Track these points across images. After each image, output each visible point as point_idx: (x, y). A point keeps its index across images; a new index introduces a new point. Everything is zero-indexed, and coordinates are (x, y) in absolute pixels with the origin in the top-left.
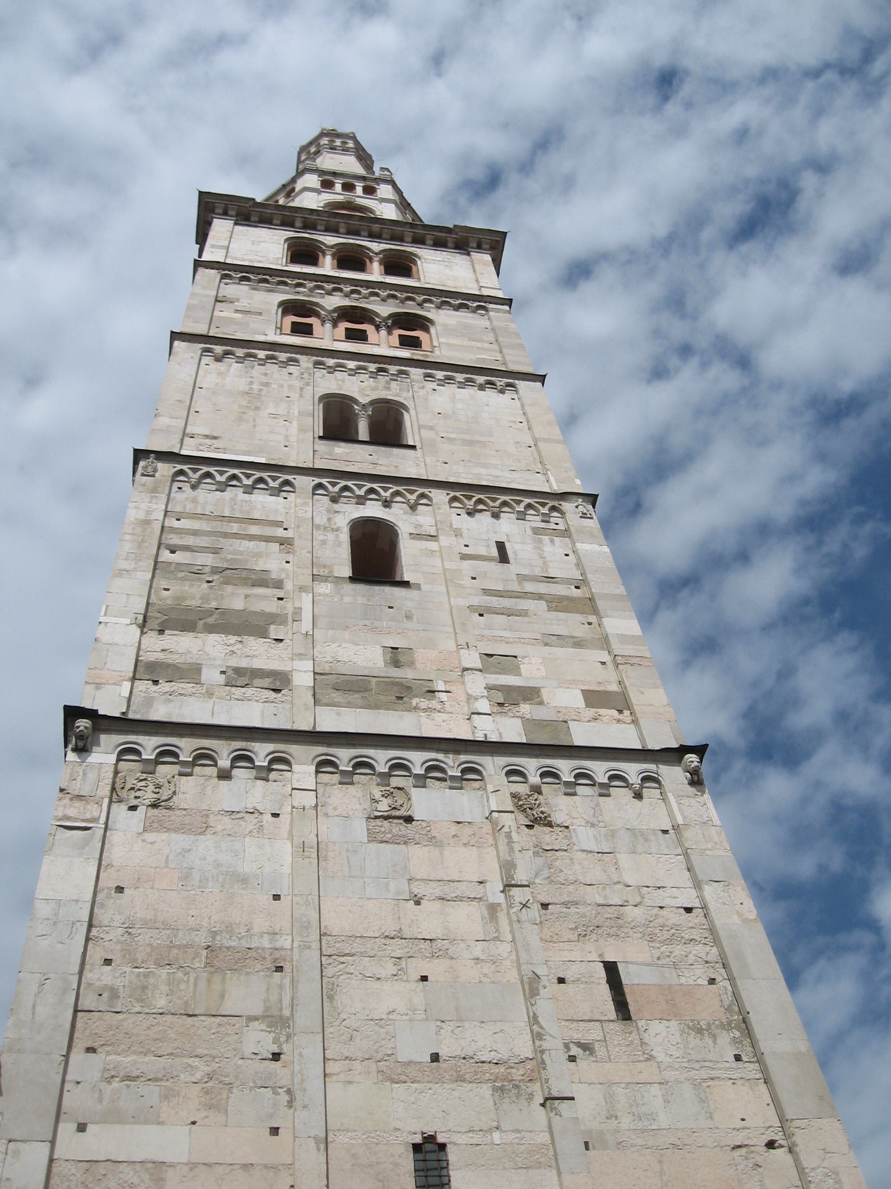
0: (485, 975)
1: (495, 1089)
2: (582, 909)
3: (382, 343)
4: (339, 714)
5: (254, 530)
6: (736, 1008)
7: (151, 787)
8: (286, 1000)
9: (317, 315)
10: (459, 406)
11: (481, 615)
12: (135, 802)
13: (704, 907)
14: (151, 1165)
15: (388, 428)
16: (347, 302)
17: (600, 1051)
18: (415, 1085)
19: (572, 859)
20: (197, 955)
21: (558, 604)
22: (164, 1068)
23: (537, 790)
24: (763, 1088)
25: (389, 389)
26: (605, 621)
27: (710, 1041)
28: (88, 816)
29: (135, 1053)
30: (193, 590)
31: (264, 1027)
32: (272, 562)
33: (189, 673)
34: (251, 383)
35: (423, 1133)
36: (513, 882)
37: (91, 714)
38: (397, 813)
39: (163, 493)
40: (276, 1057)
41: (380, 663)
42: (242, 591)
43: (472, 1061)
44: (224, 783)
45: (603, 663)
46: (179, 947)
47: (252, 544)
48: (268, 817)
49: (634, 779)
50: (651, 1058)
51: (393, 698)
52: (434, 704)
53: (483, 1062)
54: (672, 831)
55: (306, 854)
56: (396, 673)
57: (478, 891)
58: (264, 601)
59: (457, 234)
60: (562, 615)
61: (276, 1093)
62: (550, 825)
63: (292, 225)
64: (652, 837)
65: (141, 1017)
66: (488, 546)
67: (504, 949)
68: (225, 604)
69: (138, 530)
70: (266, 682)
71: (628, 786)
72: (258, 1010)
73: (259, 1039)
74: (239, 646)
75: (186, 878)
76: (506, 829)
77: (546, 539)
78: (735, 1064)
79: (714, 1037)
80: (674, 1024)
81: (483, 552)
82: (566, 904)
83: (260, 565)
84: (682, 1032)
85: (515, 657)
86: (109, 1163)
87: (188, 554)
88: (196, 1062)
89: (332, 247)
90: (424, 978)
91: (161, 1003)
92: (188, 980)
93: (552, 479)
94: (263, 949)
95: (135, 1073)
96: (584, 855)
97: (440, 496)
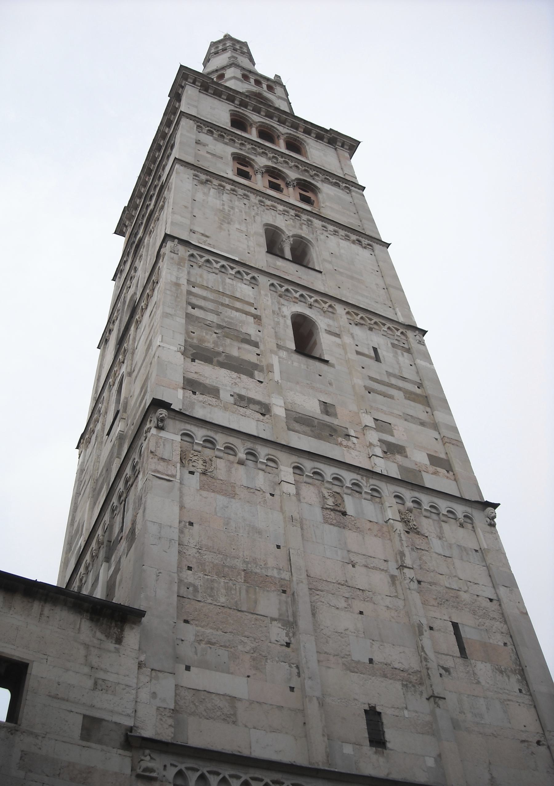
0: (393, 617)
1: (403, 685)
3: (291, 196)
4: (299, 438)
5: (238, 305)
6: (518, 663)
7: (201, 462)
8: (290, 613)
9: (252, 166)
10: (342, 251)
11: (369, 393)
12: (192, 469)
13: (499, 600)
14: (228, 698)
15: (300, 254)
16: (270, 163)
17: (454, 674)
18: (362, 675)
19: (431, 557)
20: (239, 574)
22: (229, 641)
23: (410, 510)
24: (533, 710)
25: (302, 229)
26: (436, 413)
27: (506, 678)
29: (211, 628)
31: (280, 625)
32: (250, 328)
34: (223, 205)
35: (369, 704)
36: (405, 565)
37: (166, 406)
38: (338, 509)
39: (184, 267)
40: (288, 645)
41: (318, 411)
42: (236, 344)
43: (390, 667)
44: (241, 468)
45: (437, 439)
46: (228, 567)
47: (238, 314)
49: (460, 515)
50: (478, 683)
51: (328, 434)
53: (396, 669)
54: (479, 551)
55: (294, 523)
56: (327, 419)
57: (383, 566)
58: (248, 354)
59: (331, 135)
60: (412, 403)
61: (290, 666)
62: (418, 533)
64: (470, 553)
65: (212, 607)
66: (368, 349)
67: (401, 603)
68: (228, 350)
69: (174, 289)
70: (257, 407)
72: (276, 615)
73: (277, 633)
74: (238, 380)
75: (227, 524)
76: (398, 532)
78: (519, 694)
79: (508, 677)
80: (488, 665)
81: (366, 351)
82: (431, 584)
85: (390, 424)
86: (205, 693)
87: (202, 311)
88: (245, 640)
89: (257, 123)
90: (361, 613)
91: (222, 600)
93: (399, 314)
94: (275, 578)
95: (214, 640)
96: (436, 555)
97: (340, 309)
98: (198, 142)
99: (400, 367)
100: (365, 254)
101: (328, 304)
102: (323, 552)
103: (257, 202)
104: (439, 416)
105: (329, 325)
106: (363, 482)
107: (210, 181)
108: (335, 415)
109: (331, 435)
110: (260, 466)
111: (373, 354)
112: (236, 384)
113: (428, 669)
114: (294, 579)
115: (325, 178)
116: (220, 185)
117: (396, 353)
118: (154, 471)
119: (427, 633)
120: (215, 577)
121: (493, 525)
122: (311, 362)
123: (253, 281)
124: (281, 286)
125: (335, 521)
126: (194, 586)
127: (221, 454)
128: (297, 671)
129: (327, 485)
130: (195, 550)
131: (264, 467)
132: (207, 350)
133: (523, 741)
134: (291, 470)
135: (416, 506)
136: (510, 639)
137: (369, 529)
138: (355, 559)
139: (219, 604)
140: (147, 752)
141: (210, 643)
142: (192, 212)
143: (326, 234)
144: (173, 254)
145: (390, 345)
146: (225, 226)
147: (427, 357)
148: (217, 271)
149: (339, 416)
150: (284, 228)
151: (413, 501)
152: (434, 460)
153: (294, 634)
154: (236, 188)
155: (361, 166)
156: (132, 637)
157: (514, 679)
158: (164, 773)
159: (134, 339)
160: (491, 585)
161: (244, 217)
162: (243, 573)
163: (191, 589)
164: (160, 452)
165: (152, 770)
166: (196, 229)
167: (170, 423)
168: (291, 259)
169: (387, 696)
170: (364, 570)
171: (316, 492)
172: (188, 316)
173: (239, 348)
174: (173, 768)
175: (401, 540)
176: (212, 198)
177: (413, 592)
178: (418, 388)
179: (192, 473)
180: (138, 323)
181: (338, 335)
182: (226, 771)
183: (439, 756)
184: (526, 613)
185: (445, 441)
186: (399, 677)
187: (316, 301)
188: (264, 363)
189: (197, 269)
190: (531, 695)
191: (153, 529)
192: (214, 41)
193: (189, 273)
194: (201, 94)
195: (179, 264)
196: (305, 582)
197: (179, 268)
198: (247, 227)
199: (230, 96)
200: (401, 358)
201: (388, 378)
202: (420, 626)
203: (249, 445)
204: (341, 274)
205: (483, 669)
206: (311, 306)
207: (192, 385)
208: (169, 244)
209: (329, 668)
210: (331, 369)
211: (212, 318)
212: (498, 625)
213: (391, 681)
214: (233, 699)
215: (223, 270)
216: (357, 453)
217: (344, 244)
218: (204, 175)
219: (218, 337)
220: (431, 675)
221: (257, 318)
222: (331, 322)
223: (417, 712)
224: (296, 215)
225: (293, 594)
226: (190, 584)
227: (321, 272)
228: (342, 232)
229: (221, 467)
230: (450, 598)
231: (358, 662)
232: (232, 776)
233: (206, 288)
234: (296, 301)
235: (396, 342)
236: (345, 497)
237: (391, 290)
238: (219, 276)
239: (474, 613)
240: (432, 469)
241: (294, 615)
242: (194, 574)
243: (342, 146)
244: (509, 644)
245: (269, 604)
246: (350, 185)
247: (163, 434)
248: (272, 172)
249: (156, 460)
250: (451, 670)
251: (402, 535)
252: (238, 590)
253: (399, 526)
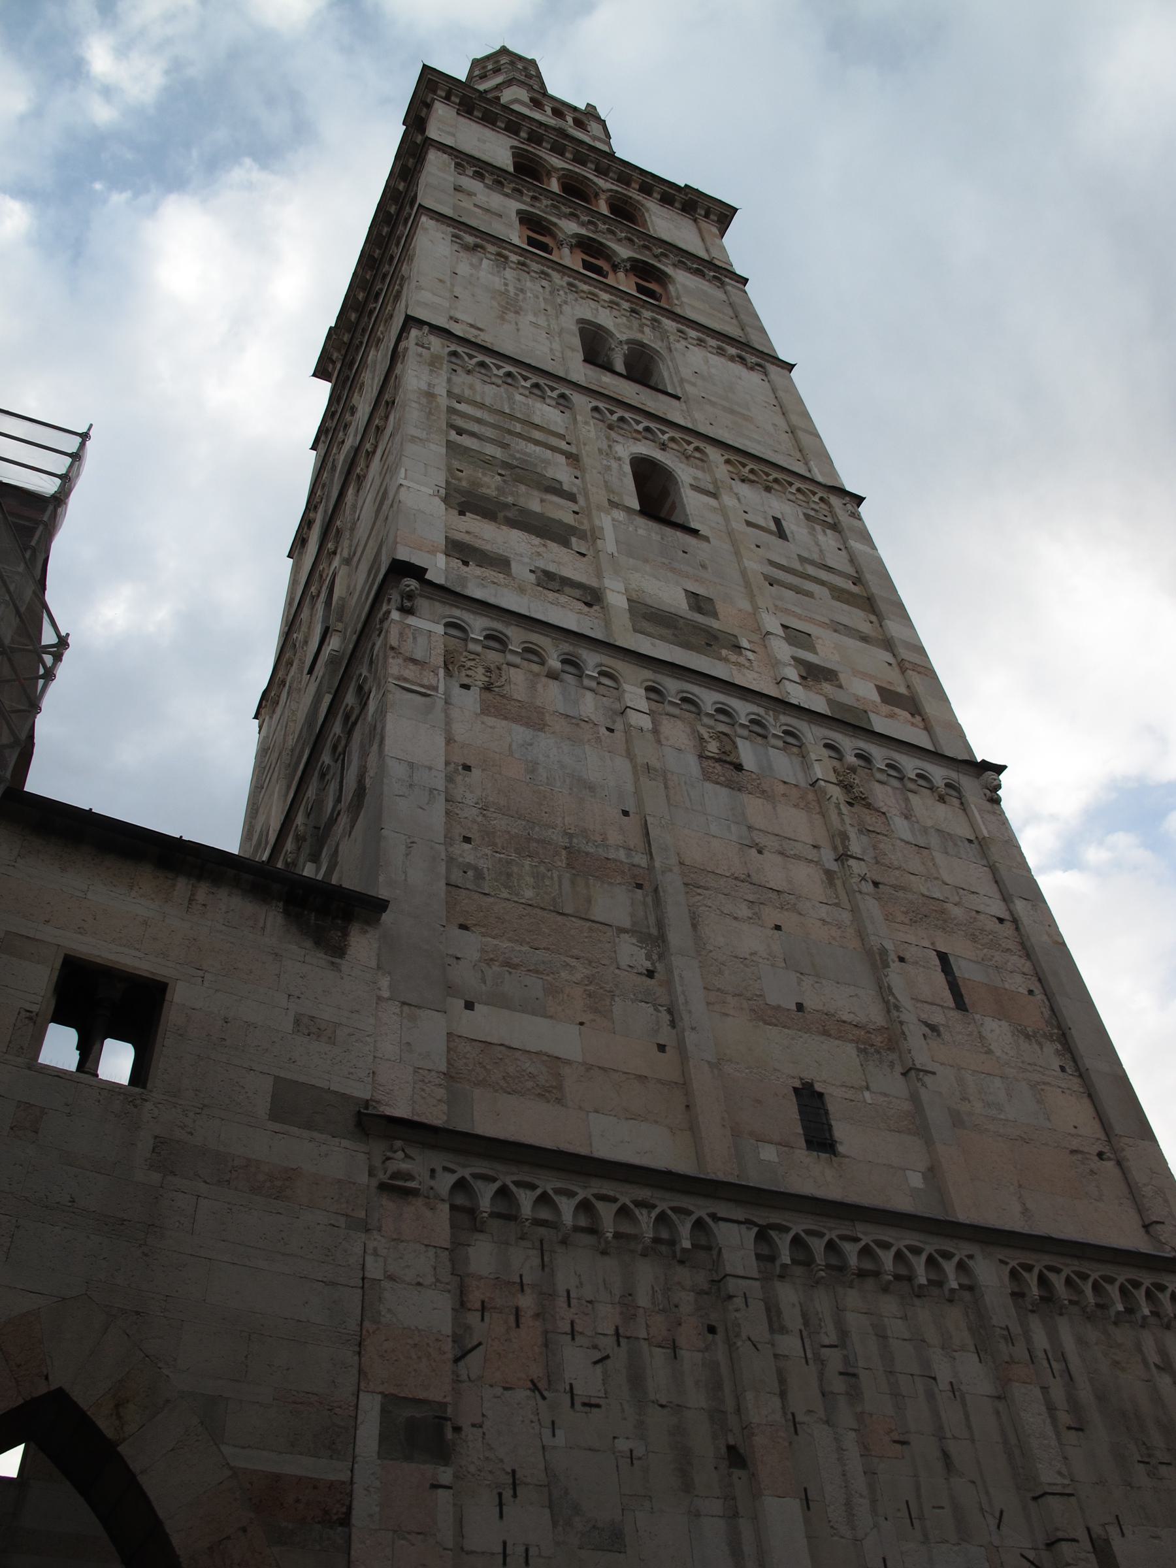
0: (834, 938)
1: (859, 1050)
2: (910, 896)
5: (537, 435)
6: (1055, 1023)
7: (481, 670)
8: (652, 920)
9: (553, 236)
10: (713, 371)
12: (466, 681)
13: (1015, 921)
14: (545, 1058)
16: (583, 231)
18: (786, 1031)
21: (839, 594)
22: (544, 962)
23: (853, 770)
24: (1086, 1101)
25: (643, 332)
27: (1036, 1047)
28: (425, 682)
29: (510, 940)
31: (634, 941)
32: (561, 472)
34: (506, 285)
35: (801, 1079)
37: (418, 572)
38: (728, 759)
39: (441, 369)
40: (650, 974)
44: (554, 686)
45: (890, 664)
46: (537, 841)
47: (538, 449)
48: (603, 731)
50: (989, 1052)
52: (742, 660)
53: (844, 1022)
54: (976, 842)
57: (812, 854)
58: (561, 511)
59: (686, 195)
60: (845, 607)
61: (656, 1010)
62: (868, 806)
63: (516, 133)
64: (960, 843)
66: (765, 518)
67: (846, 917)
68: (522, 502)
69: (424, 401)
70: (578, 593)
71: (932, 788)
72: (627, 924)
73: (631, 953)
74: (541, 549)
76: (834, 800)
78: (1061, 1074)
80: (1004, 1023)
81: (762, 523)
82: (895, 887)
83: (550, 473)
86: (502, 1048)
87: (475, 440)
88: (573, 962)
90: (778, 928)
91: (529, 893)
92: (552, 878)
94: (621, 862)
95: (516, 961)
96: (903, 844)
97: (714, 455)
98: (458, 189)
99: (821, 551)
100: (755, 377)
101: (692, 446)
102: (702, 826)
103: (565, 284)
104: (893, 628)
105: (695, 478)
106: (769, 719)
107: (482, 247)
108: (715, 615)
110: (586, 682)
111: (773, 527)
112: (539, 554)
113: (901, 1023)
114: (657, 864)
115: (680, 261)
116: (499, 254)
117: (814, 529)
118: (398, 679)
119: (895, 965)
120: (514, 856)
121: (997, 801)
122: (668, 531)
123: (562, 401)
124: (612, 413)
125: (723, 779)
126: (476, 869)
127: (517, 660)
128: (668, 1017)
129: (706, 720)
130: (475, 811)
131: (593, 684)
132: (486, 498)
133: (1073, 1152)
134: (642, 692)
135: (862, 763)
136: (1038, 984)
137: (784, 795)
139: (523, 901)
140: (398, 1144)
141: (507, 964)
142: (452, 291)
143: (684, 343)
144: (420, 349)
145: (801, 516)
146: (510, 316)
147: (866, 538)
148: (499, 382)
149: (720, 617)
150: (612, 329)
151: (857, 755)
152: (887, 695)
153: (661, 956)
154: (528, 261)
155: (738, 246)
156: (362, 946)
157: (1050, 1048)
158: (432, 1183)
159: (354, 506)
160: (998, 896)
161: (543, 305)
162: (564, 852)
163: (470, 873)
164: (407, 648)
165: (409, 1177)
166: (459, 316)
167: (422, 604)
168: (624, 373)
169: (833, 1067)
170: (779, 859)
171: (688, 730)
172: (450, 445)
173: (542, 501)
174: (447, 1175)
175: (840, 814)
176: (484, 272)
177: (867, 897)
178: (854, 584)
179: (466, 687)
180: (360, 479)
181: (714, 495)
182: (548, 1183)
183: (931, 1169)
184: (1064, 944)
185: (903, 666)
186: (850, 1037)
187: (672, 439)
188: (586, 526)
189: (464, 375)
190: (1081, 1076)
191: (396, 770)
192: (479, 57)
193: (449, 380)
194: (461, 119)
195: (432, 364)
196: (676, 869)
197: (431, 371)
198: (548, 320)
199: (512, 124)
200: (821, 537)
201: (802, 565)
202: (883, 952)
203: (566, 647)
204: (713, 404)
205: (997, 1031)
206: (663, 447)
207: (459, 550)
208: (414, 333)
209: (727, 1015)
210: (705, 545)
211: (491, 450)
212: (1016, 960)
213: (837, 1042)
214: (555, 1061)
215: (509, 381)
216: (756, 675)
217: (716, 360)
218: (472, 238)
219: (504, 481)
220: (907, 1033)
221: (573, 459)
222: (699, 474)
223: (886, 1095)
224: (633, 311)
225: (656, 890)
226: (469, 865)
227: (678, 398)
228: (713, 342)
229: (517, 681)
230: (929, 913)
231: (778, 1008)
232: (559, 1192)
233: (481, 406)
234: (637, 436)
235: (812, 513)
236: (738, 740)
237: (800, 434)
238: (502, 389)
239: (974, 938)
240: (885, 709)
241: (660, 924)
242: (475, 849)
243: (707, 216)
244: (1036, 992)
245: (614, 905)
246: (724, 276)
247: (411, 620)
248: (585, 245)
249: (400, 661)
251: (842, 806)
252: (556, 878)
253: (836, 792)
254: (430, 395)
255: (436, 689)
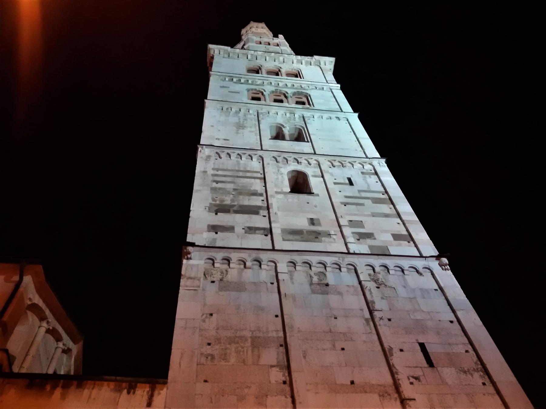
1: (380, 396)
21: (377, 201)
28: (195, 285)
30: (227, 198)
31: (278, 369)
33: (231, 229)
34: (239, 119)
42: (247, 197)
45: (398, 223)
46: (238, 337)
47: (248, 180)
52: (331, 240)
70: (262, 231)
72: (274, 362)
76: (368, 288)
77: (367, 176)
81: (342, 181)
84: (457, 372)
90: (343, 349)
92: (244, 351)
109: (317, 238)
136: (470, 346)
137: (347, 291)
138: (336, 313)
145: (360, 173)
152: (397, 237)
163: (209, 358)
172: (213, 189)
179: (213, 282)
205: (449, 373)
210: (317, 197)
226: (209, 355)
239: (438, 333)
242: (212, 347)
250: (421, 378)
254: (205, 172)
255: (199, 287)
